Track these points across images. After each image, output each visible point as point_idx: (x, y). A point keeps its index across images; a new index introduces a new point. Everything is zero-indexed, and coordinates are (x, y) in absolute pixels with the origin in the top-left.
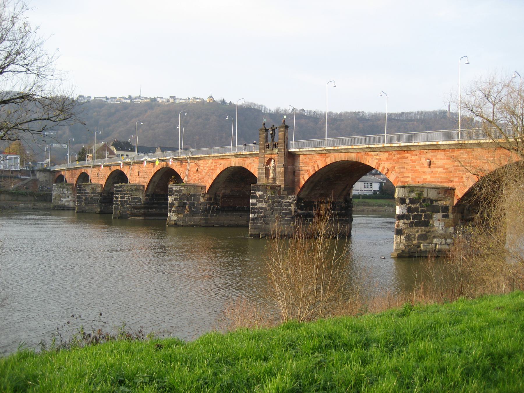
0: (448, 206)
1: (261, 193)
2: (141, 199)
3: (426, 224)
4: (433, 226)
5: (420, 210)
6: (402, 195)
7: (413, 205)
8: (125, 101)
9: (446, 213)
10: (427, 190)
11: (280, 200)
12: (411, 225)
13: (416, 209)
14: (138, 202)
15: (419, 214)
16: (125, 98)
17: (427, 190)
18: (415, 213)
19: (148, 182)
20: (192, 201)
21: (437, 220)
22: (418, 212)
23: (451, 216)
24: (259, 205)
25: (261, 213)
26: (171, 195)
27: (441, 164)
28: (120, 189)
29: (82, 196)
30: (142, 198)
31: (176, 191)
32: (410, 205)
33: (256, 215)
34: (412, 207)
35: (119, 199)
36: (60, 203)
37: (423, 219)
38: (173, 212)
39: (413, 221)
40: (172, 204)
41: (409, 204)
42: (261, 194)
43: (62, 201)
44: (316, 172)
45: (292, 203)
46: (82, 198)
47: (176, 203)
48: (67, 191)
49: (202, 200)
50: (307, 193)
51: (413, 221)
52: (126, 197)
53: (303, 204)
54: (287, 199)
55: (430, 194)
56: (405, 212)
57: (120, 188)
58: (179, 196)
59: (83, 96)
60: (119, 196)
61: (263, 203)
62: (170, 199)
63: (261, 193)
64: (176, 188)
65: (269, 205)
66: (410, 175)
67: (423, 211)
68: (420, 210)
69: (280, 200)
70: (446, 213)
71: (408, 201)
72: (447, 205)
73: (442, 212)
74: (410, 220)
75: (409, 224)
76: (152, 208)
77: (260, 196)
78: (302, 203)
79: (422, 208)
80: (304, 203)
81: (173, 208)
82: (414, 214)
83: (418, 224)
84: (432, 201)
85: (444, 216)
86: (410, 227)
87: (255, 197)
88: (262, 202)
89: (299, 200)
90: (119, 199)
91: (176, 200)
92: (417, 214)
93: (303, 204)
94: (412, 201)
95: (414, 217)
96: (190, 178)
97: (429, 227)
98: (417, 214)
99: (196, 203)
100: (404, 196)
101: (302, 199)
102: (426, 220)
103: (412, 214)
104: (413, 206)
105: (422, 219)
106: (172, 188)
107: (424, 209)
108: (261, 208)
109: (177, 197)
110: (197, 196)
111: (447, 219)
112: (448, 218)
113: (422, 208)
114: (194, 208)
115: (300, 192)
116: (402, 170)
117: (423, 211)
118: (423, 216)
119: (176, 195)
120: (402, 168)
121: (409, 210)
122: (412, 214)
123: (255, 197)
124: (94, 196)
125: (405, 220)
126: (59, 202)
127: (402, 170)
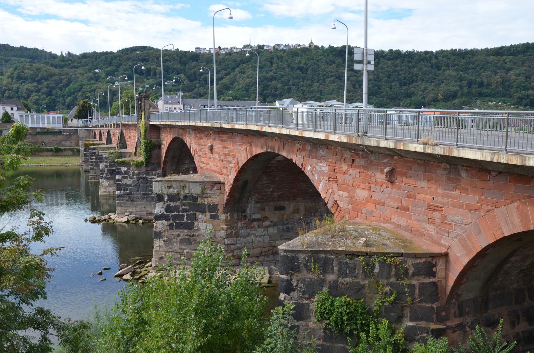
0: (217, 205)
3: (190, 226)
4: (198, 230)
5: (181, 209)
6: (159, 191)
7: (172, 203)
9: (215, 213)
10: (189, 184)
12: (171, 226)
13: (176, 209)
15: (181, 213)
17: (189, 184)
18: (176, 213)
21: (204, 222)
22: (179, 212)
23: (222, 217)
25: (127, 189)
31: (106, 158)
32: (169, 203)
33: (122, 192)
34: (171, 205)
37: (185, 220)
38: (104, 179)
39: (173, 222)
41: (167, 202)
42: (125, 170)
47: (106, 169)
51: (173, 222)
54: (152, 175)
55: (192, 190)
56: (163, 211)
57: (94, 150)
58: (109, 163)
59: (199, 48)
60: (94, 157)
61: (129, 179)
65: (133, 182)
67: (184, 211)
68: (181, 209)
70: (215, 213)
71: (166, 198)
72: (216, 203)
73: (209, 212)
74: (170, 221)
75: (169, 225)
77: (125, 171)
79: (184, 207)
81: (104, 175)
82: (174, 214)
83: (178, 227)
84: (195, 198)
85: (212, 217)
86: (170, 229)
88: (124, 177)
90: (94, 161)
91: (106, 167)
92: (177, 213)
94: (172, 198)
95: (175, 218)
97: (193, 230)
98: (177, 213)
100: (161, 192)
102: (189, 221)
103: (172, 214)
104: (172, 204)
105: (184, 220)
106: (102, 155)
107: (186, 208)
108: (127, 185)
109: (108, 164)
111: (216, 220)
112: (218, 219)
113: (184, 207)
117: (184, 211)
118: (185, 217)
119: (106, 162)
121: (168, 209)
122: (172, 214)
125: (164, 221)
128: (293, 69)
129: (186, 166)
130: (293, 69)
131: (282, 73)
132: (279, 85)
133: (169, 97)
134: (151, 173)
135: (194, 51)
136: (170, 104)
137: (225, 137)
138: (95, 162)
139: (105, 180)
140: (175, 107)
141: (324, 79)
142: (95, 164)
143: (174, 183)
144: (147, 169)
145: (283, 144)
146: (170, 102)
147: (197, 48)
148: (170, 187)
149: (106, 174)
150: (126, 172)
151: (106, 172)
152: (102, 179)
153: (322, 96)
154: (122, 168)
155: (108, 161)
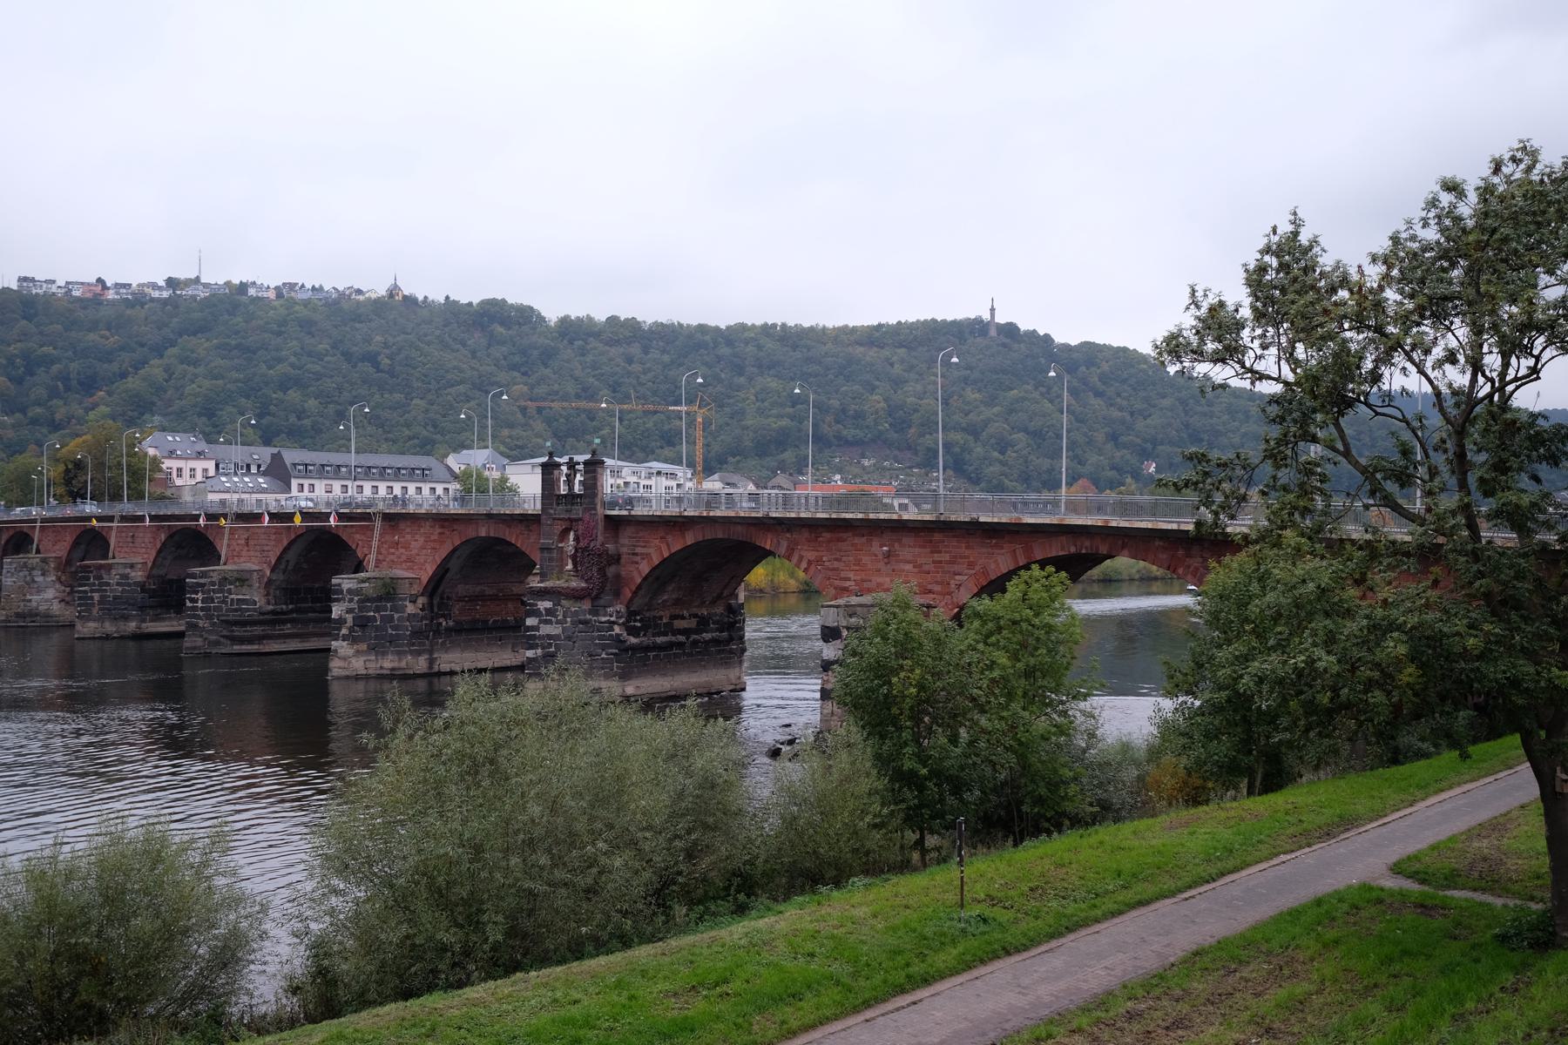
1: (548, 604)
2: (255, 603)
8: (156, 294)
11: (588, 617)
14: (248, 610)
16: (154, 286)
19: (273, 562)
20: (388, 613)
24: (546, 630)
26: (338, 600)
27: (909, 557)
28: (202, 581)
29: (92, 591)
30: (257, 599)
31: (350, 591)
33: (539, 651)
35: (200, 605)
36: (25, 606)
38: (343, 640)
40: (341, 621)
43: (30, 601)
44: (665, 559)
45: (614, 623)
46: (92, 598)
47: (349, 618)
48: (43, 575)
49: (411, 609)
50: (647, 600)
52: (217, 598)
53: (639, 624)
54: (605, 616)
57: (201, 577)
59: (33, 280)
60: (200, 596)
62: (337, 611)
63: (548, 604)
64: (351, 585)
65: (564, 629)
66: (851, 575)
69: (588, 617)
76: (284, 622)
77: (546, 609)
78: (635, 621)
80: (640, 621)
81: (344, 631)
87: (536, 613)
89: (631, 614)
90: (200, 605)
91: (349, 611)
93: (639, 624)
96: (380, 557)
99: (396, 616)
101: (635, 613)
106: (339, 585)
108: (549, 637)
110: (401, 599)
114: (393, 628)
115: (631, 600)
116: (836, 565)
119: (351, 601)
120: (836, 560)
123: (536, 613)
124: (122, 592)
126: (22, 604)
127: (836, 565)
128: (347, 356)
129: (665, 597)
130: (347, 356)
131: (318, 368)
132: (312, 403)
133: (170, 438)
134: (601, 612)
135: (14, 286)
136: (179, 458)
137: (937, 536)
138: (202, 609)
139: (345, 643)
140: (193, 467)
141: (439, 389)
142: (201, 614)
143: (859, 609)
144: (596, 604)
145: (1120, 542)
146: (179, 453)
147: (23, 279)
148: (851, 616)
149: (351, 629)
150: (549, 612)
151: (350, 622)
152: (336, 640)
153: (438, 437)
154: (539, 603)
155: (356, 598)
